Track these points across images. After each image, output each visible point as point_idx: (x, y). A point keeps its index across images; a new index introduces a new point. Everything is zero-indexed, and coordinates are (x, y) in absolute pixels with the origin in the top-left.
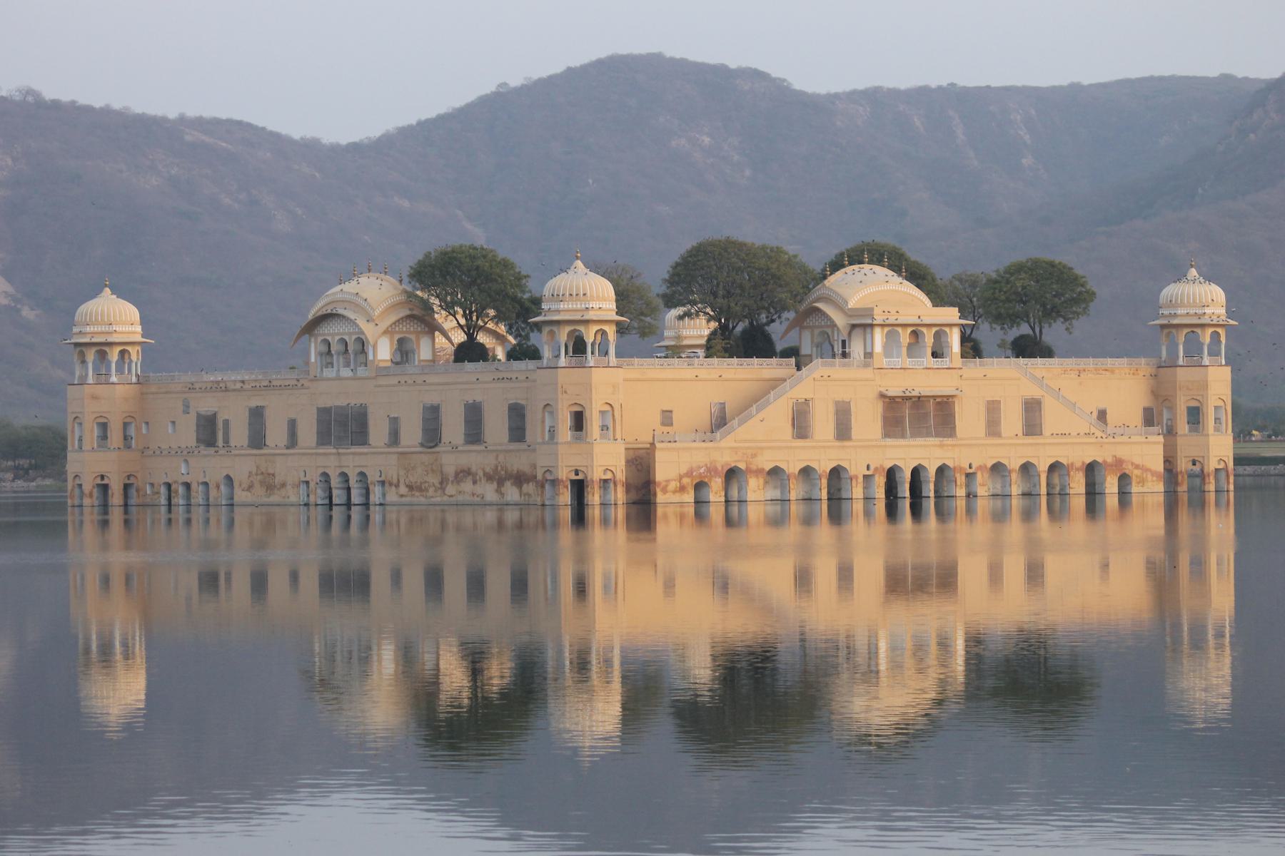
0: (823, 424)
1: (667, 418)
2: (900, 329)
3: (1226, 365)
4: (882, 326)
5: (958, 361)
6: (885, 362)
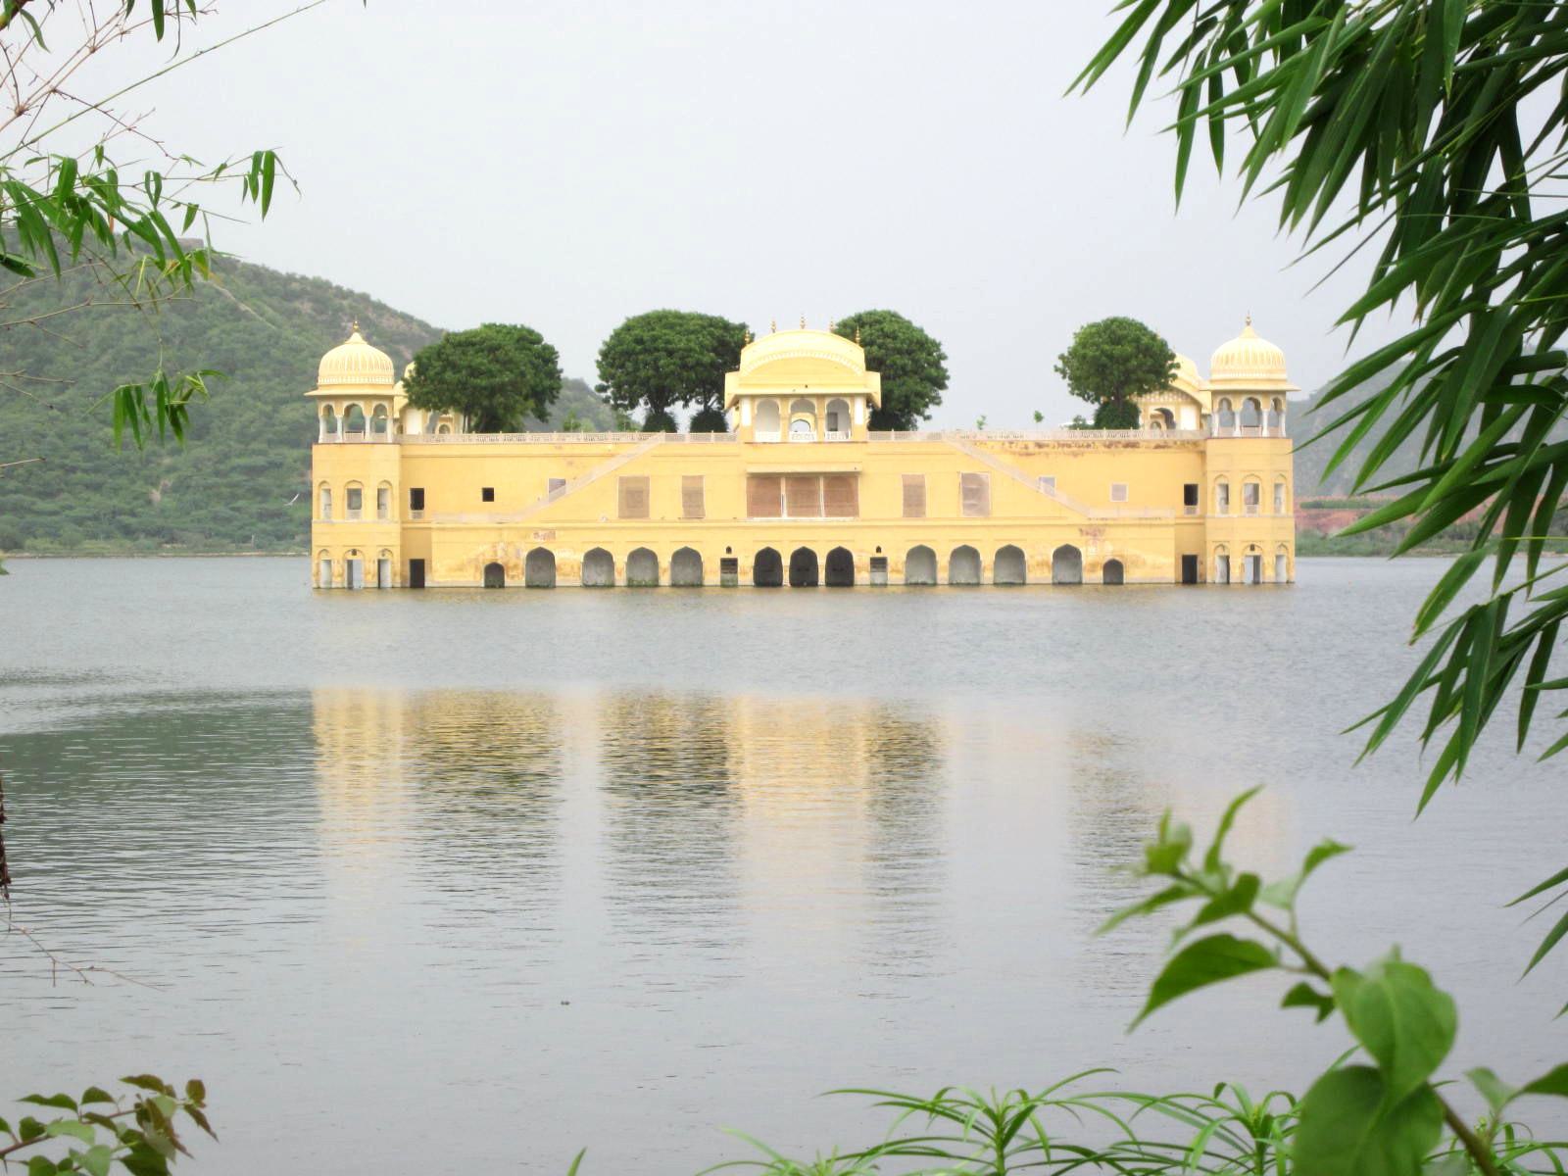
0: (665, 502)
1: (488, 495)
2: (778, 401)
3: (1288, 438)
4: (753, 397)
5: (866, 435)
6: (761, 436)
